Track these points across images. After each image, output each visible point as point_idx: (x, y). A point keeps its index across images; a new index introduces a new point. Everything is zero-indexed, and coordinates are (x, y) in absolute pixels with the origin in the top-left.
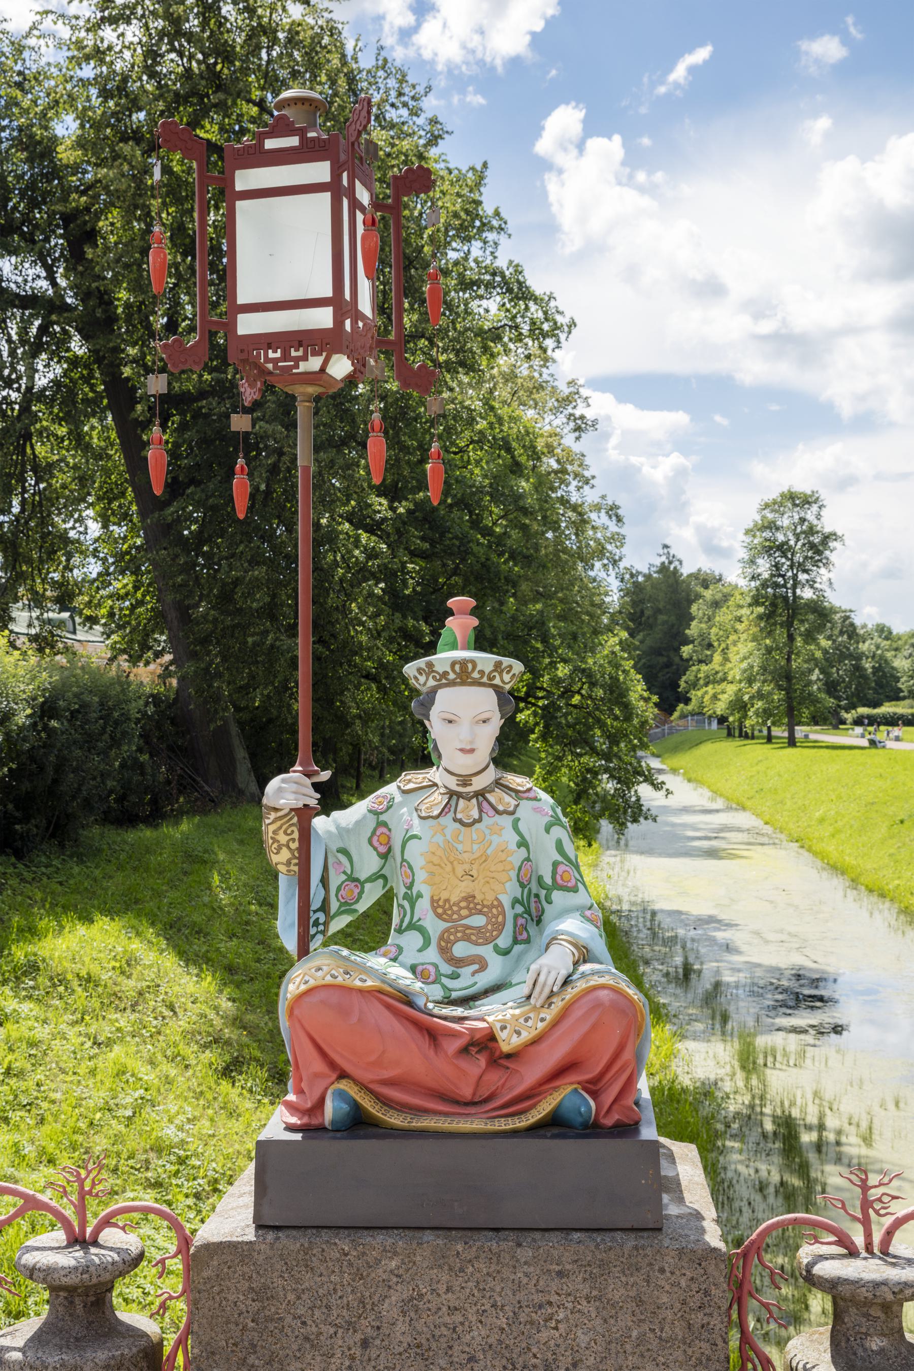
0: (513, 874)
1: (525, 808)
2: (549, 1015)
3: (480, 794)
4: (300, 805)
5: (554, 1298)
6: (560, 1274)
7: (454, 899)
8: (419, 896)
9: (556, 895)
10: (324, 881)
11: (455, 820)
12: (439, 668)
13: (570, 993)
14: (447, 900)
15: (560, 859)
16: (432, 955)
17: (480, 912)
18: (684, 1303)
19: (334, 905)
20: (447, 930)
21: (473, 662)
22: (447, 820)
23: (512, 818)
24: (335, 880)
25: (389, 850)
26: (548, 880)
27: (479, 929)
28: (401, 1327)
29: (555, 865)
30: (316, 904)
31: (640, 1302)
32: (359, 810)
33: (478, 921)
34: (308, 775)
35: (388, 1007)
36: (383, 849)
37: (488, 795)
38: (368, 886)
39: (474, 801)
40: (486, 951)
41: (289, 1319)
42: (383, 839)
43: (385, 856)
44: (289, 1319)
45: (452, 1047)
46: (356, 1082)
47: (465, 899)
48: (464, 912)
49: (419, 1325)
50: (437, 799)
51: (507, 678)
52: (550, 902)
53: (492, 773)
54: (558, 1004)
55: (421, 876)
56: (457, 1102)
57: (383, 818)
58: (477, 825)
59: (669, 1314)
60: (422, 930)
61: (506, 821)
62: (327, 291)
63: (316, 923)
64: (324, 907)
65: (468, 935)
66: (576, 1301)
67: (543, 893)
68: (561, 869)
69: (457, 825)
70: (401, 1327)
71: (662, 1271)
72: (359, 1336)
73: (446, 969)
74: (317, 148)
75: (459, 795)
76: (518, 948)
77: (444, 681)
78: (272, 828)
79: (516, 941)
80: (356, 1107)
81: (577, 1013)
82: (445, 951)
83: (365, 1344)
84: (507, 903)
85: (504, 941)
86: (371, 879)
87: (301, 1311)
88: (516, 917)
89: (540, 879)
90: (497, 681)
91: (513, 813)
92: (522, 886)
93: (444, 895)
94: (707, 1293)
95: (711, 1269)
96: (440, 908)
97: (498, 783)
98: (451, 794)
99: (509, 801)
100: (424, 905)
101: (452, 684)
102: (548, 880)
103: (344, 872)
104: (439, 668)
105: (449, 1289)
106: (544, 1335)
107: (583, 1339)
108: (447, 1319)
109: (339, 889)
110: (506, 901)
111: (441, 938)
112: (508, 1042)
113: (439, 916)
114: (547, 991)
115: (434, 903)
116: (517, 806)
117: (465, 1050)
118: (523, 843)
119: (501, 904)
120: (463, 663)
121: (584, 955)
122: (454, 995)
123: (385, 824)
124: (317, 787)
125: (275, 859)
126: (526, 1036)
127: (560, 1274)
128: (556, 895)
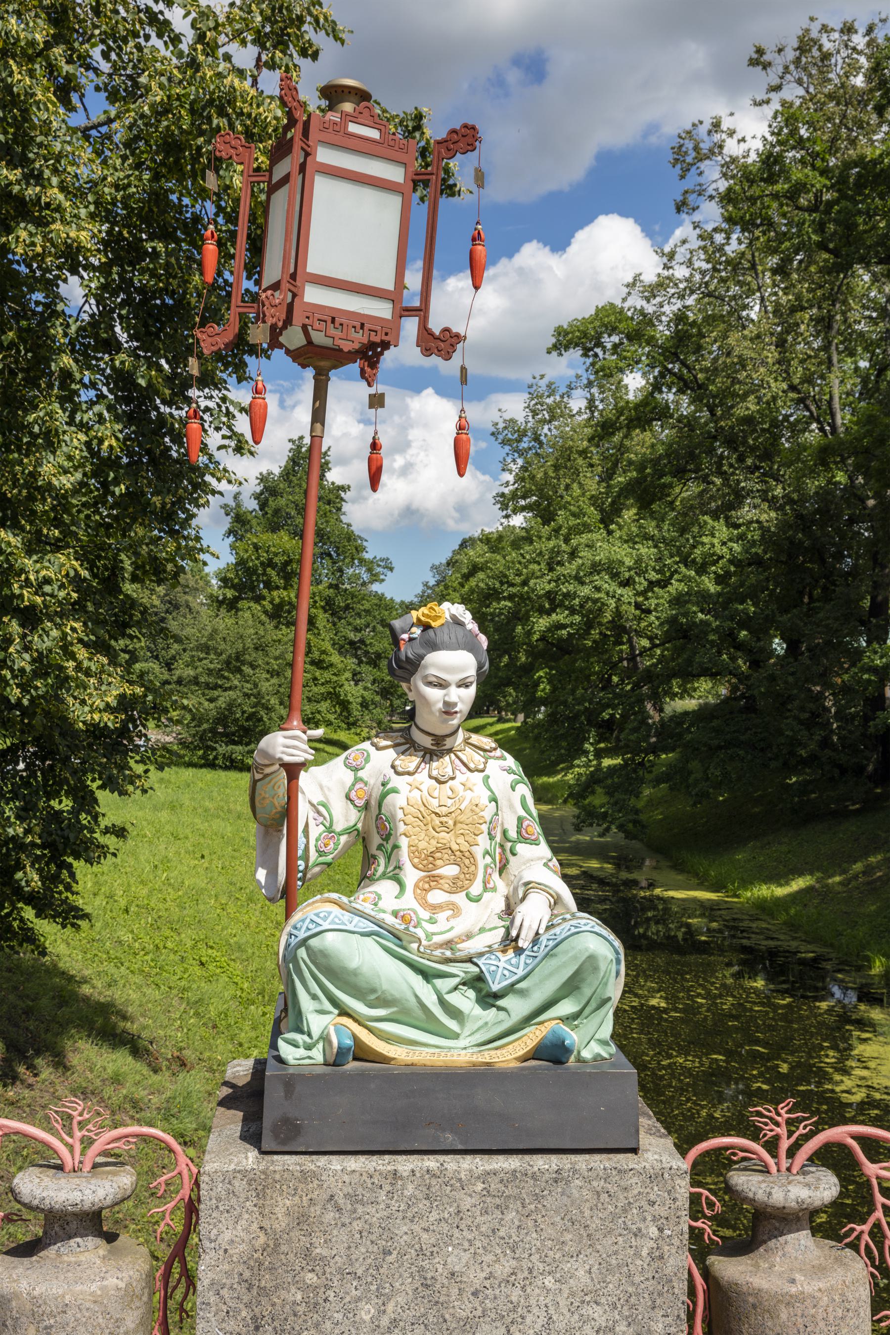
1: (493, 767)
9: (520, 848)
11: (430, 777)
15: (522, 813)
16: (409, 901)
20: (421, 879)
23: (482, 774)
26: (513, 834)
29: (520, 820)
37: (459, 753)
39: (447, 758)
40: (460, 899)
48: (439, 862)
52: (514, 854)
57: (360, 774)
62: (388, 283)
67: (509, 845)
68: (525, 824)
73: (424, 914)
74: (396, 148)
79: (486, 889)
88: (486, 867)
89: (504, 832)
91: (483, 771)
102: (513, 834)
103: (322, 823)
109: (317, 840)
110: (478, 851)
111: (416, 886)
116: (485, 763)
118: (494, 799)
122: (437, 939)
128: (520, 848)
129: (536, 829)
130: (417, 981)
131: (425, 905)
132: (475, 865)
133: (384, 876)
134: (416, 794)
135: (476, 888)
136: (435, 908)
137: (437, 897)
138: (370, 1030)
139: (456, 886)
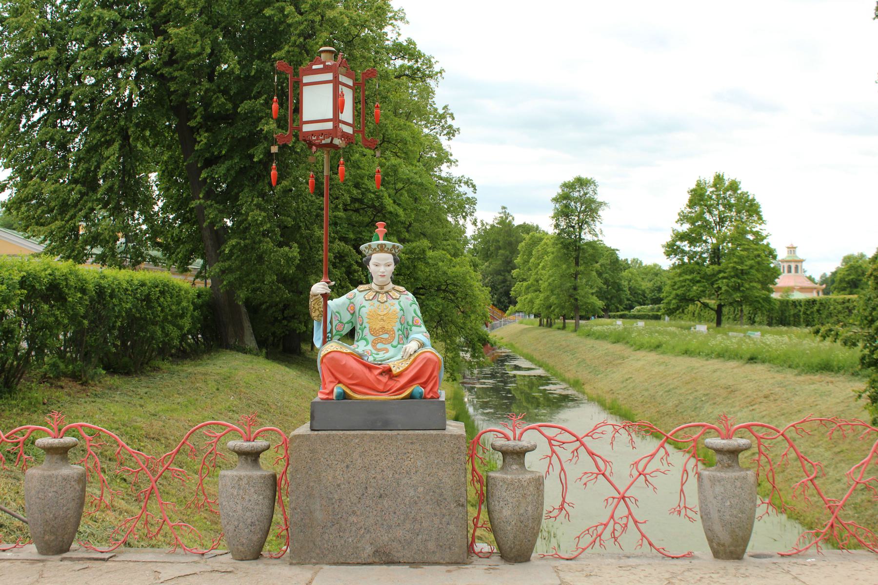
0: (398, 320)
2: (409, 362)
3: (387, 292)
4: (324, 292)
5: (410, 451)
6: (412, 443)
7: (377, 328)
8: (365, 327)
9: (414, 328)
10: (331, 322)
12: (373, 247)
13: (416, 354)
14: (375, 329)
16: (369, 347)
17: (387, 333)
18: (452, 451)
19: (334, 332)
21: (385, 245)
22: (375, 301)
24: (335, 323)
25: (354, 312)
26: (411, 323)
27: (386, 339)
28: (359, 461)
29: (413, 317)
30: (328, 330)
31: (438, 452)
32: (343, 298)
33: (386, 336)
34: (328, 283)
35: (355, 359)
36: (352, 312)
38: (346, 325)
40: (388, 346)
41: (322, 459)
42: (352, 308)
43: (353, 314)
44: (322, 459)
45: (377, 372)
46: (344, 384)
47: (381, 328)
48: (381, 333)
49: (366, 461)
50: (371, 295)
51: (397, 251)
53: (391, 285)
54: (412, 358)
55: (366, 320)
56: (378, 392)
58: (386, 303)
59: (447, 455)
60: (365, 339)
61: (396, 302)
63: (328, 337)
64: (331, 332)
65: (382, 341)
66: (417, 452)
69: (379, 303)
70: (359, 461)
71: (445, 442)
72: (345, 464)
73: (374, 351)
75: (379, 293)
76: (399, 346)
77: (375, 251)
78: (313, 303)
79: (399, 343)
80: (344, 392)
81: (418, 361)
82: (374, 345)
83: (347, 467)
84: (396, 331)
85: (395, 343)
86: (347, 323)
87: (326, 457)
88: (399, 335)
89: (408, 322)
90: (393, 252)
92: (401, 324)
93: (374, 327)
94: (459, 448)
95: (461, 441)
96: (373, 332)
97: (393, 289)
98: (377, 292)
99: (397, 295)
100: (366, 331)
101: (377, 252)
102: (411, 323)
104: (373, 247)
105: (375, 449)
106: (406, 463)
107: (419, 464)
108: (375, 458)
110: (396, 329)
112: (395, 371)
113: (372, 334)
114: (409, 355)
115: (370, 329)
117: (381, 374)
118: (402, 310)
119: (394, 330)
120: (382, 245)
121: (422, 345)
123: (353, 303)
124: (330, 287)
125: (313, 315)
126: (401, 369)
127: (412, 443)
128: (414, 328)
129: (421, 322)
130: (366, 371)
131: (377, 349)
132: (394, 333)
133: (362, 339)
134: (372, 307)
135: (395, 343)
136: (379, 350)
137: (380, 346)
138: (349, 388)
139: (388, 341)
